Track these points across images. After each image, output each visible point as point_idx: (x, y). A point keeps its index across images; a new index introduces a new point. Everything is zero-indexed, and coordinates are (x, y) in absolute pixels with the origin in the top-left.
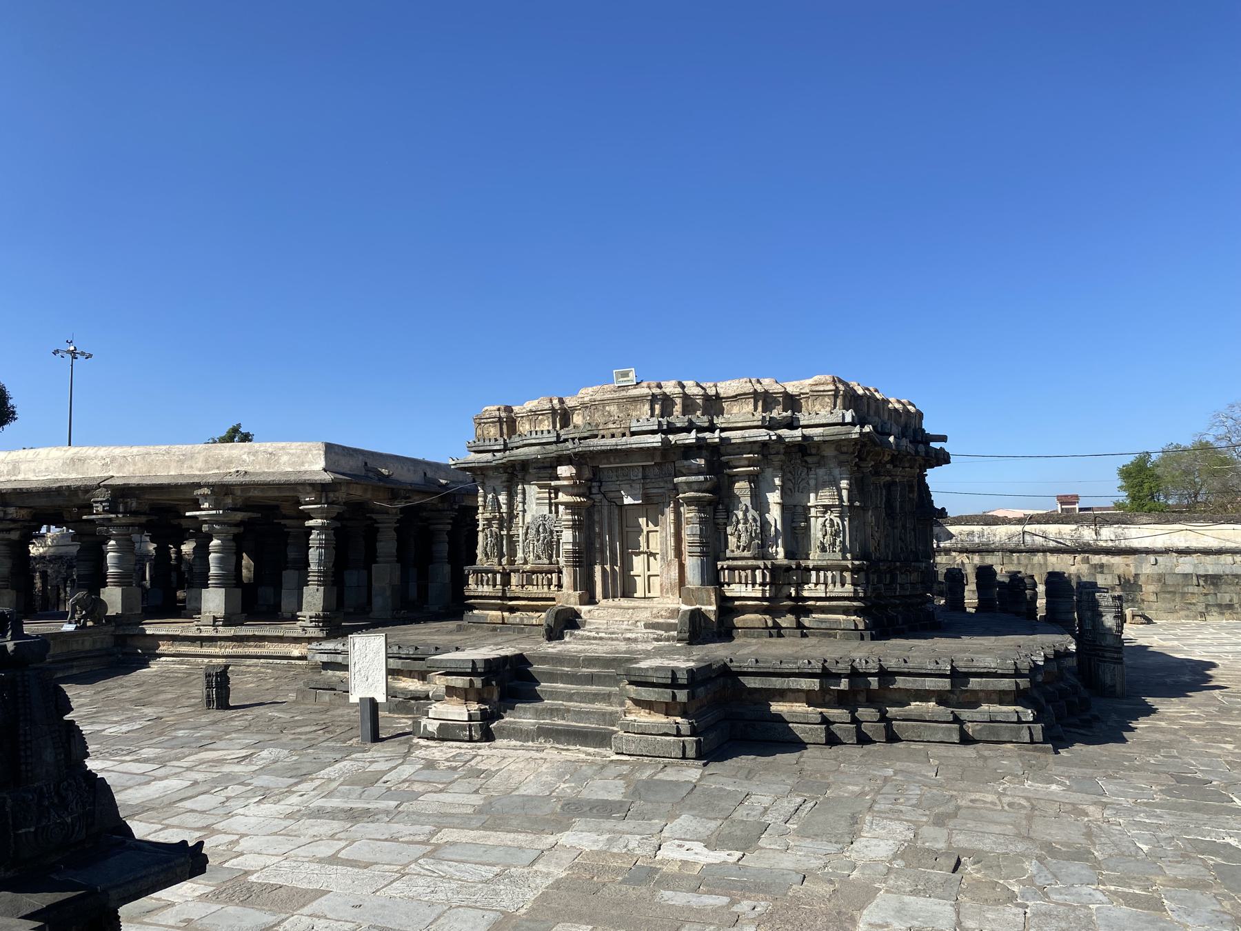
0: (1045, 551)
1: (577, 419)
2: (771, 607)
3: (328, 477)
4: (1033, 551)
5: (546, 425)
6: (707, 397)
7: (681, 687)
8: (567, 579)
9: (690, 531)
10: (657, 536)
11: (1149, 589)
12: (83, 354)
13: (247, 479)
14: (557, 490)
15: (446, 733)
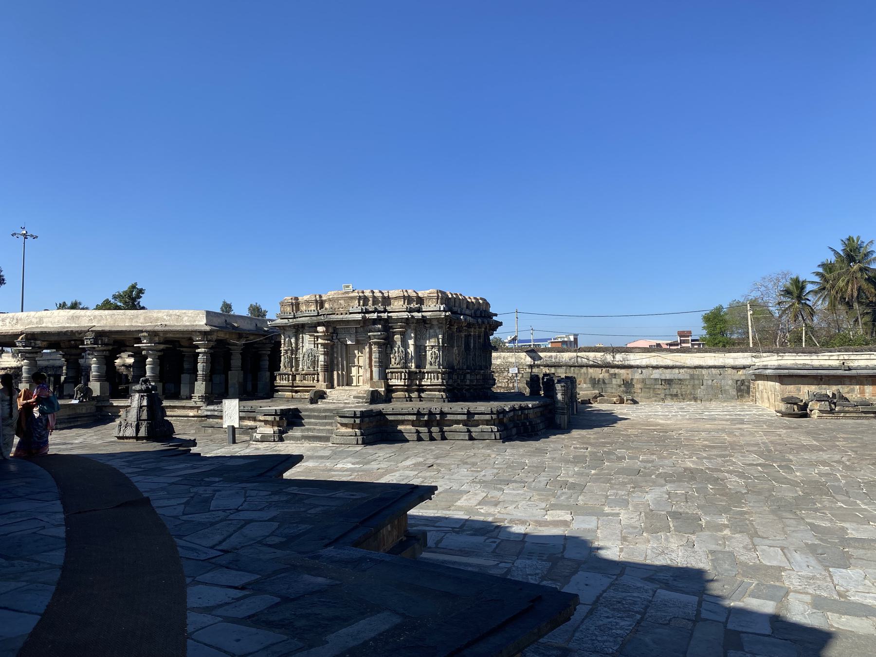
0: (587, 366)
1: (327, 305)
2: (408, 389)
3: (208, 328)
4: (581, 366)
5: (313, 308)
6: (384, 298)
7: (358, 417)
8: (321, 378)
9: (375, 356)
10: (362, 358)
11: (638, 386)
12: (32, 236)
13: (167, 328)
14: (318, 337)
15: (264, 439)
